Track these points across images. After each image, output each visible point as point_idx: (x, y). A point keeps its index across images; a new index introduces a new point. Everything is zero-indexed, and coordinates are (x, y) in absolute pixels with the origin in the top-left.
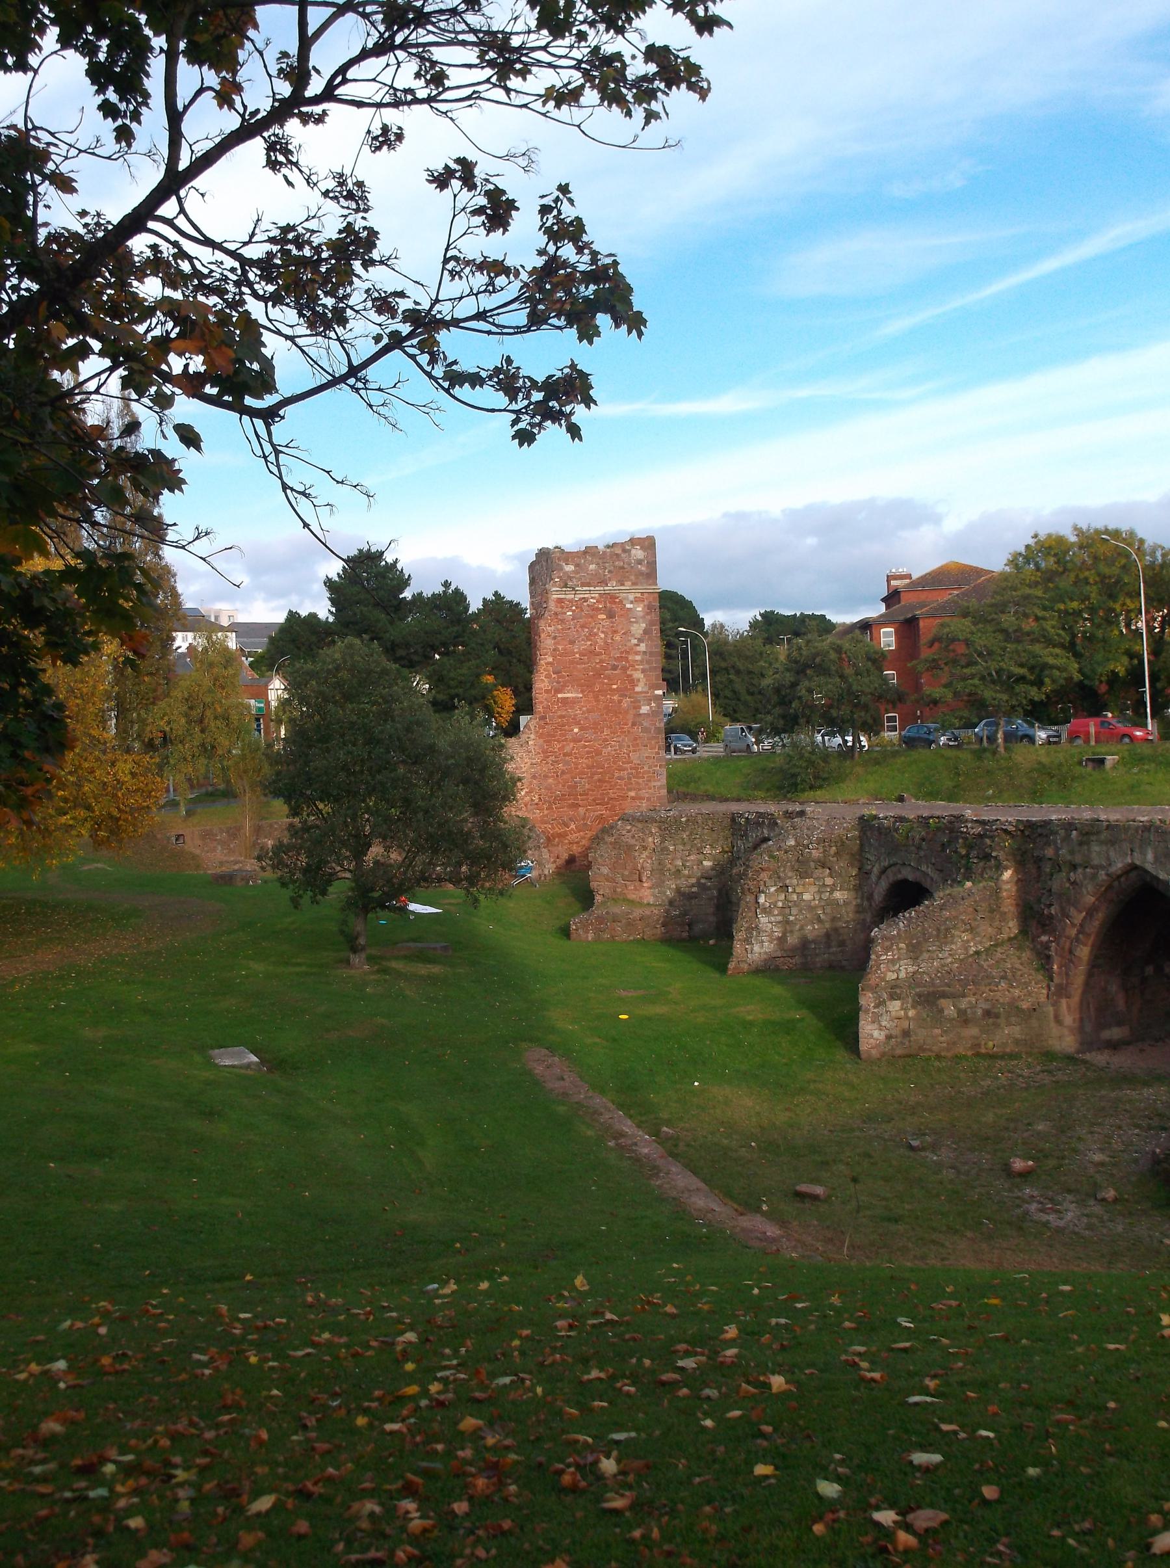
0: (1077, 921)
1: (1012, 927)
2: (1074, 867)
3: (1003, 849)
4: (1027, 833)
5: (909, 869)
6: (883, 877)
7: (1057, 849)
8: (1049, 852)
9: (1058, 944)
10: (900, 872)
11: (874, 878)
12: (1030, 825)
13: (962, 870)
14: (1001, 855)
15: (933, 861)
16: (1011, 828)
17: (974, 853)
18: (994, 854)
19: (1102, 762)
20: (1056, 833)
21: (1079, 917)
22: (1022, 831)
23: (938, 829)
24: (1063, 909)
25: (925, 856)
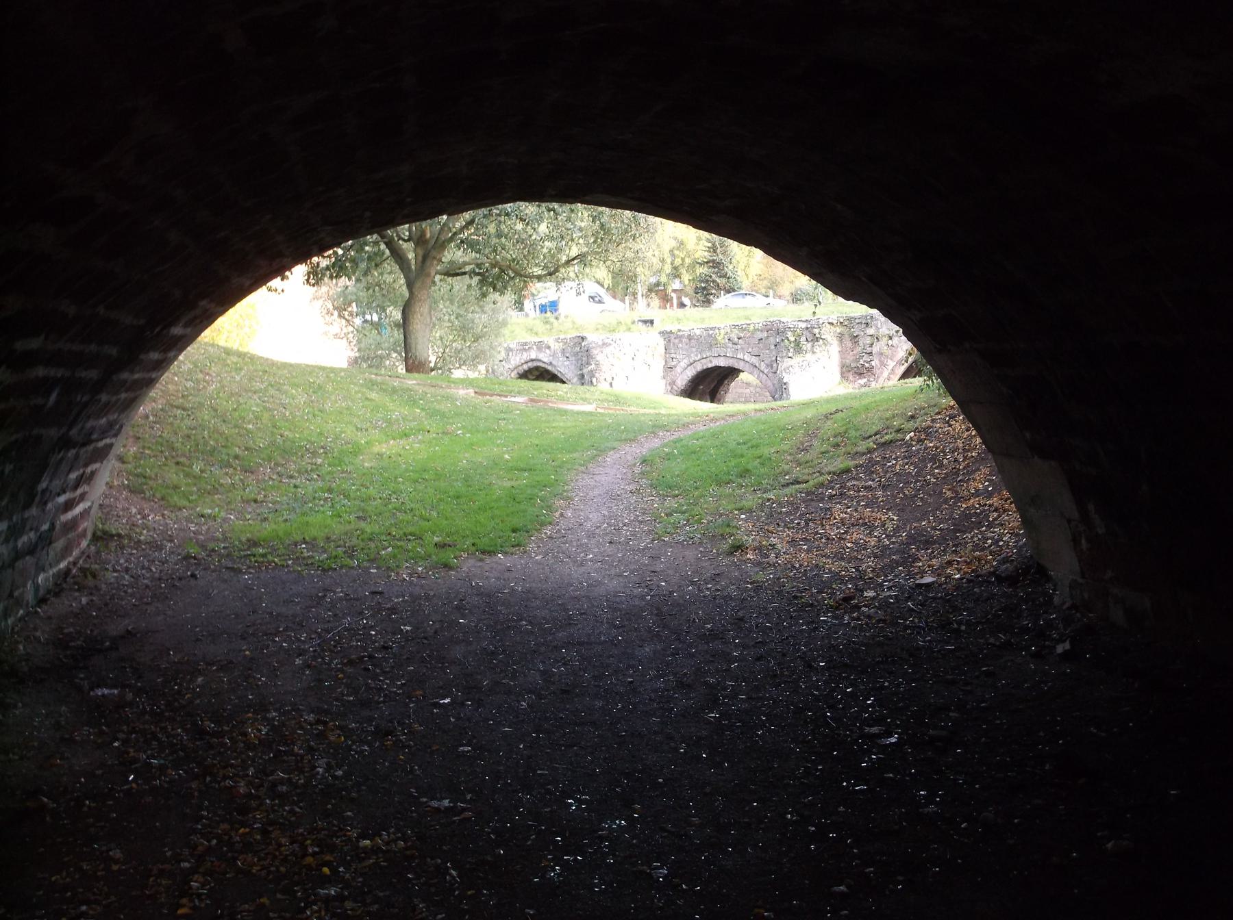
0: (890, 368)
1: (838, 375)
2: (891, 338)
3: (829, 334)
4: (846, 323)
5: (722, 358)
6: (689, 367)
7: (878, 329)
8: (871, 331)
9: (877, 382)
10: (711, 362)
11: (679, 369)
12: (850, 319)
13: (792, 350)
14: (829, 339)
15: (750, 350)
16: (835, 322)
17: (803, 339)
18: (822, 337)
19: (652, 322)
20: (878, 320)
21: (891, 364)
22: (841, 323)
23: (755, 330)
24: (880, 361)
25: (742, 348)
